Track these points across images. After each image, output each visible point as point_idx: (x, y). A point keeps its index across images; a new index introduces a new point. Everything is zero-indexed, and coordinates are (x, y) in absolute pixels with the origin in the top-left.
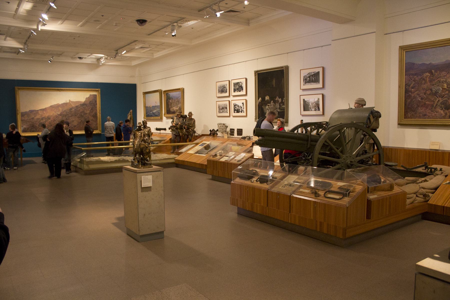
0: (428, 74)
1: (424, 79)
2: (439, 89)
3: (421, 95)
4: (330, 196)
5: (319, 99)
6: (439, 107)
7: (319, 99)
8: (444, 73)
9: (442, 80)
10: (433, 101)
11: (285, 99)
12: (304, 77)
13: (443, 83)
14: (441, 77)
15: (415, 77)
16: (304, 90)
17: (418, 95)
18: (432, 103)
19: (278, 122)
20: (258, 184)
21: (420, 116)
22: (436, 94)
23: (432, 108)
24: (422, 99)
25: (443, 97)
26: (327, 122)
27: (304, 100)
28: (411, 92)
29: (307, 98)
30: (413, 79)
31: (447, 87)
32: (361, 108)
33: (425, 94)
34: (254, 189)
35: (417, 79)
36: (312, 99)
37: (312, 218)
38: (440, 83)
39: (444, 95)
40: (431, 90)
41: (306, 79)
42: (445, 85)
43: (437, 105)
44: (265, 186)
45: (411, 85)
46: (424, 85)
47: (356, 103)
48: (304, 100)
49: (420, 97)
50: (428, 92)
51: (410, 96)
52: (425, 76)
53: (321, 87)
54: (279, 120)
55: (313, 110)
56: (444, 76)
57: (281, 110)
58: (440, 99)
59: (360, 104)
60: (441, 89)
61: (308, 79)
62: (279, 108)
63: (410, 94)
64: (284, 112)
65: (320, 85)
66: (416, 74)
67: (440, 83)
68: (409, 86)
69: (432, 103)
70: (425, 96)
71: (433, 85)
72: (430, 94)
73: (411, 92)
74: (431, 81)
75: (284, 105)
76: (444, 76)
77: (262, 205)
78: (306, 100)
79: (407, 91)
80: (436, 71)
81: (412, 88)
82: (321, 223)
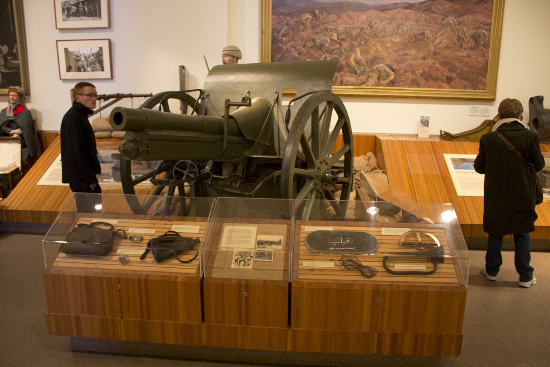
0: (308, 16)
1: (302, 24)
2: (327, 40)
3: (298, 47)
4: (398, 267)
5: (101, 49)
7: (101, 49)
8: (333, 17)
9: (330, 27)
11: (19, 45)
12: (64, 4)
13: (331, 31)
14: (328, 22)
15: (288, 18)
16: (63, 30)
17: (294, 47)
19: (11, 93)
20: (151, 267)
22: (320, 47)
24: (299, 54)
25: (330, 52)
26: (201, 91)
27: (66, 50)
28: (282, 42)
29: (73, 47)
30: (285, 22)
31: (338, 39)
32: (235, 63)
33: (304, 46)
34: (143, 283)
35: (291, 22)
36: (85, 48)
37: (366, 328)
38: (327, 30)
39: (333, 50)
40: (314, 40)
41: (68, 9)
44: (174, 268)
45: (282, 32)
46: (303, 33)
47: (224, 55)
48: (66, 50)
49: (297, 50)
50: (310, 44)
51: (279, 49)
52: (304, 18)
53: (106, 25)
54: (14, 90)
55: (89, 69)
56: (334, 21)
57: (11, 69)
58: (328, 55)
59: (233, 57)
60: (329, 40)
61: (74, 8)
62: (5, 66)
63: (280, 45)
64: (18, 74)
65: (103, 22)
66: (289, 14)
68: (279, 33)
70: (304, 50)
71: (317, 33)
72: (311, 47)
73: (282, 42)
74: (313, 27)
75: (16, 58)
76: (334, 21)
77: (182, 320)
78: (70, 50)
79: (274, 41)
80: (321, 13)
81: (284, 35)
82: (394, 337)
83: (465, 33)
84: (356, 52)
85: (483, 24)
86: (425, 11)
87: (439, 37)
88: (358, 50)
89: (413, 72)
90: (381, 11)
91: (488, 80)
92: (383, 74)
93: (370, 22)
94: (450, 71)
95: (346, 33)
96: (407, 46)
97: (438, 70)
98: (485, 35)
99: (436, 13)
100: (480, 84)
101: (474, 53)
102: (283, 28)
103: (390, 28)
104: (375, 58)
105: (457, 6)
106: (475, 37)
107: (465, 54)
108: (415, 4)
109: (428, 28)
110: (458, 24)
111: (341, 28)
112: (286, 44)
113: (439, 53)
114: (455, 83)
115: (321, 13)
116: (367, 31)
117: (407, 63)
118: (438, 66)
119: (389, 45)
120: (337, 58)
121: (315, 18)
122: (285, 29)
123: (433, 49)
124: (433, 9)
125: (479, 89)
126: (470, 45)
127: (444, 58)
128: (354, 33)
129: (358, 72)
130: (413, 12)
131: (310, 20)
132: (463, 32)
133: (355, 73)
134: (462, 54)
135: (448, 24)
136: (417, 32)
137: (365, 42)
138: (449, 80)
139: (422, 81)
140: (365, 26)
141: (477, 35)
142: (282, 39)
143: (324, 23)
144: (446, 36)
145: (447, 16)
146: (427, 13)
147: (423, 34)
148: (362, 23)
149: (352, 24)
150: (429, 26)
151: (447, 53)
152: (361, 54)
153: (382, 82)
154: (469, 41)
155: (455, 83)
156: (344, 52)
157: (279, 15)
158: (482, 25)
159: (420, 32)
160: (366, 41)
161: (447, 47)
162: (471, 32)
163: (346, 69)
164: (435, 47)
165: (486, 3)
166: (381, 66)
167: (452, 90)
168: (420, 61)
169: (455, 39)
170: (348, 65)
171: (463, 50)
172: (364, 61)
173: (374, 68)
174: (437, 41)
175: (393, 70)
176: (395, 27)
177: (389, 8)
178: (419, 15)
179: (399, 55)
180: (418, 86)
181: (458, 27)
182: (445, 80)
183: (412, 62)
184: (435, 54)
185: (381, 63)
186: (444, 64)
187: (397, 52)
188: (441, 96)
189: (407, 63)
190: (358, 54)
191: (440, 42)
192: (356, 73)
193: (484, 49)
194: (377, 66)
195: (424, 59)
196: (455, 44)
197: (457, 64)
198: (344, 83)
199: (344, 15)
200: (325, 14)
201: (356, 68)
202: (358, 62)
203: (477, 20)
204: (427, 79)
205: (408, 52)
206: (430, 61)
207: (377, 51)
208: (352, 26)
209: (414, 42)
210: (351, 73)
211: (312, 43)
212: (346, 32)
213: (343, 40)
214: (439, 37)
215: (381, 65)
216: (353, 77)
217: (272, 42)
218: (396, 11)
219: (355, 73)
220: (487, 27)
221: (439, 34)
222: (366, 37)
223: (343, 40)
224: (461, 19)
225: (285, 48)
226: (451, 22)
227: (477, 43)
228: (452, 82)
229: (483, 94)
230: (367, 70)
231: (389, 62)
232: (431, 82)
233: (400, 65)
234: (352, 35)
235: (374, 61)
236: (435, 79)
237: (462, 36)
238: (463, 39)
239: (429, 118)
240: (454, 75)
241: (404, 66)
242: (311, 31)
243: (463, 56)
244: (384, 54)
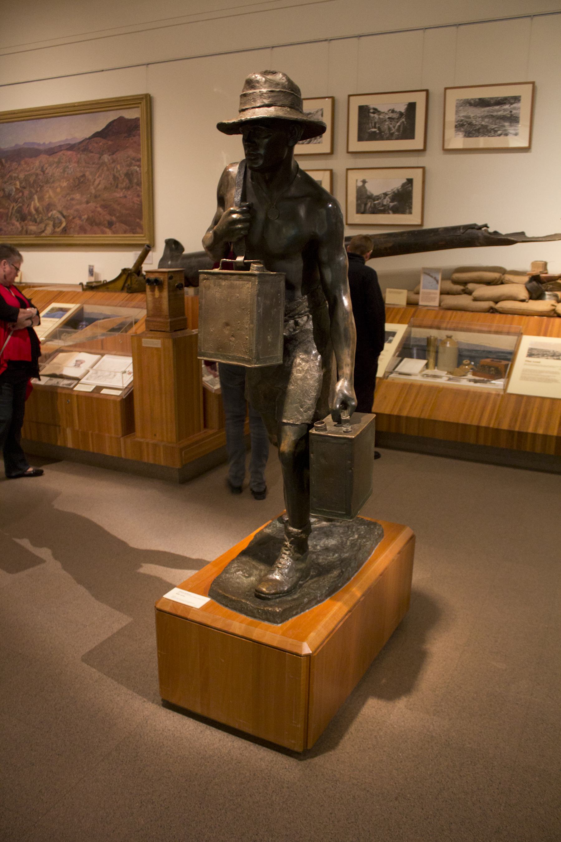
2: (12, 190)
6: (14, 218)
8: (14, 164)
14: (12, 170)
23: (7, 220)
25: (16, 201)
42: (18, 183)
43: (12, 213)
58: (15, 204)
67: (12, 179)
71: (5, 183)
80: (6, 162)
83: (119, 171)
84: (34, 200)
85: (134, 160)
86: (84, 150)
87: (98, 177)
89: (80, 218)
90: (50, 155)
91: (145, 222)
92: (57, 221)
93: (42, 167)
94: (110, 215)
95: (26, 180)
96: (72, 190)
97: (100, 214)
98: (137, 172)
99: (92, 152)
100: (137, 228)
101: (129, 193)
103: (57, 172)
104: (48, 205)
105: (110, 143)
106: (129, 175)
107: (122, 194)
108: (75, 144)
109: (88, 169)
110: (112, 162)
111: (22, 176)
113: (99, 196)
114: (115, 227)
115: (6, 162)
116: (41, 177)
117: (75, 208)
118: (99, 209)
119: (59, 190)
120: (20, 207)
123: (93, 191)
124: (90, 148)
125: (138, 233)
126: (124, 184)
127: (104, 200)
128: (32, 180)
129: (38, 220)
130: (75, 153)
132: (118, 171)
133: (35, 221)
134: (118, 195)
135: (104, 163)
136: (79, 174)
137: (40, 189)
138: (110, 224)
139: (88, 228)
140: (39, 171)
141: (130, 173)
143: (10, 172)
144: (103, 176)
145: (102, 155)
146: (86, 153)
147: (84, 176)
148: (36, 170)
149: (29, 171)
150: (89, 167)
151: (106, 195)
152: (38, 201)
153: (58, 230)
154: (123, 179)
155: (115, 227)
156: (26, 200)
158: (133, 162)
159: (82, 174)
160: (42, 187)
161: (105, 188)
162: (124, 170)
163: (29, 217)
164: (95, 188)
165: (134, 136)
166: (54, 213)
167: (113, 235)
168: (84, 206)
169: (111, 179)
170: (30, 213)
171: (119, 190)
172: (41, 209)
173: (50, 215)
174: (97, 182)
175: (64, 217)
176: (62, 171)
177: (56, 151)
178: (79, 156)
179: (68, 200)
180: (85, 232)
181: (113, 165)
182: (107, 225)
183: (78, 207)
184: (96, 197)
185: (55, 210)
186: (104, 207)
187: (65, 197)
188: (107, 242)
189: (75, 208)
190: (36, 202)
191: (99, 184)
192: (36, 222)
193: (138, 188)
194: (51, 213)
195: (88, 202)
196: (111, 184)
197: (116, 206)
198: (28, 232)
199: (23, 162)
201: (36, 217)
202: (37, 210)
203: (128, 157)
204: (91, 224)
205: (74, 196)
206: (92, 205)
207: (50, 197)
208: (30, 172)
209: (78, 185)
210: (33, 222)
212: (26, 179)
213: (24, 188)
214: (98, 177)
215: (54, 212)
216: (34, 225)
218: (61, 153)
219: (35, 221)
220: (138, 163)
221: (97, 175)
223: (24, 188)
224: (114, 156)
226: (106, 160)
227: (131, 181)
228: (113, 226)
229: (140, 238)
230: (45, 218)
231: (60, 208)
232: (95, 228)
233: (69, 211)
235: (49, 207)
236: (99, 224)
237: (117, 175)
238: (118, 178)
239: (93, 266)
240: (114, 218)
241: (72, 211)
243: (120, 198)
244: (55, 200)
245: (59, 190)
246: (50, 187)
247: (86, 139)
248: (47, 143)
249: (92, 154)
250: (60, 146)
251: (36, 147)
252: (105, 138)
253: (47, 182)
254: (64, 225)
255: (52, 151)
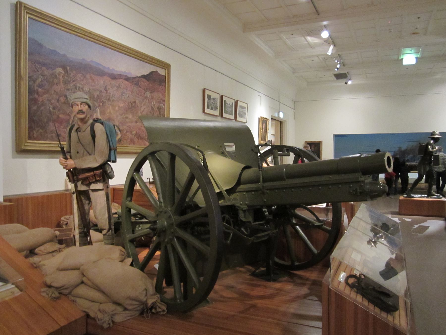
0: (60, 70)
1: (56, 77)
8: (80, 76)
10: (69, 115)
15: (44, 68)
18: (67, 117)
21: (52, 137)
24: (54, 108)
28: (38, 93)
35: (46, 73)
49: (51, 104)
63: (36, 96)
69: (67, 117)
70: (58, 104)
71: (68, 90)
84: (96, 112)
88: (98, 110)
90: (112, 79)
93: (106, 87)
99: (141, 87)
102: (39, 78)
105: (151, 85)
106: (159, 109)
112: (42, 96)
116: (104, 94)
117: (128, 124)
119: (117, 108)
121: (66, 74)
122: (40, 80)
128: (96, 94)
131: (62, 75)
132: (154, 105)
135: (146, 97)
137: (103, 104)
139: (136, 140)
142: (37, 90)
147: (135, 102)
149: (94, 86)
150: (138, 97)
157: (35, 63)
162: (157, 105)
164: (141, 113)
168: (134, 124)
174: (142, 109)
176: (120, 94)
179: (123, 118)
180: (134, 143)
181: (151, 100)
183: (130, 124)
187: (122, 115)
189: (128, 124)
200: (74, 72)
205: (128, 116)
207: (110, 112)
208: (94, 88)
211: (65, 99)
217: (28, 92)
222: (103, 99)
225: (41, 100)
227: (160, 112)
232: (140, 141)
234: (94, 97)
237: (153, 107)
241: (125, 127)
242: (63, 86)
245: (117, 108)
246: (111, 105)
247: (137, 77)
248: (111, 68)
249: (140, 89)
250: (120, 75)
251: (101, 68)
252: (148, 80)
253: (109, 100)
254: (119, 136)
255: (114, 77)
